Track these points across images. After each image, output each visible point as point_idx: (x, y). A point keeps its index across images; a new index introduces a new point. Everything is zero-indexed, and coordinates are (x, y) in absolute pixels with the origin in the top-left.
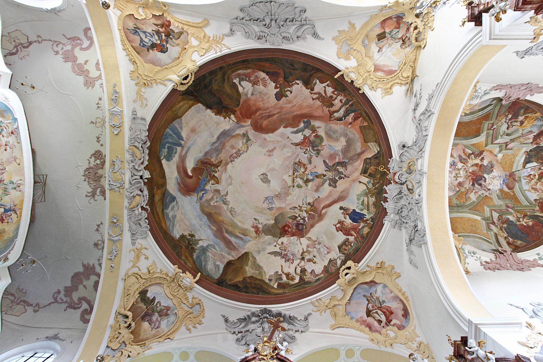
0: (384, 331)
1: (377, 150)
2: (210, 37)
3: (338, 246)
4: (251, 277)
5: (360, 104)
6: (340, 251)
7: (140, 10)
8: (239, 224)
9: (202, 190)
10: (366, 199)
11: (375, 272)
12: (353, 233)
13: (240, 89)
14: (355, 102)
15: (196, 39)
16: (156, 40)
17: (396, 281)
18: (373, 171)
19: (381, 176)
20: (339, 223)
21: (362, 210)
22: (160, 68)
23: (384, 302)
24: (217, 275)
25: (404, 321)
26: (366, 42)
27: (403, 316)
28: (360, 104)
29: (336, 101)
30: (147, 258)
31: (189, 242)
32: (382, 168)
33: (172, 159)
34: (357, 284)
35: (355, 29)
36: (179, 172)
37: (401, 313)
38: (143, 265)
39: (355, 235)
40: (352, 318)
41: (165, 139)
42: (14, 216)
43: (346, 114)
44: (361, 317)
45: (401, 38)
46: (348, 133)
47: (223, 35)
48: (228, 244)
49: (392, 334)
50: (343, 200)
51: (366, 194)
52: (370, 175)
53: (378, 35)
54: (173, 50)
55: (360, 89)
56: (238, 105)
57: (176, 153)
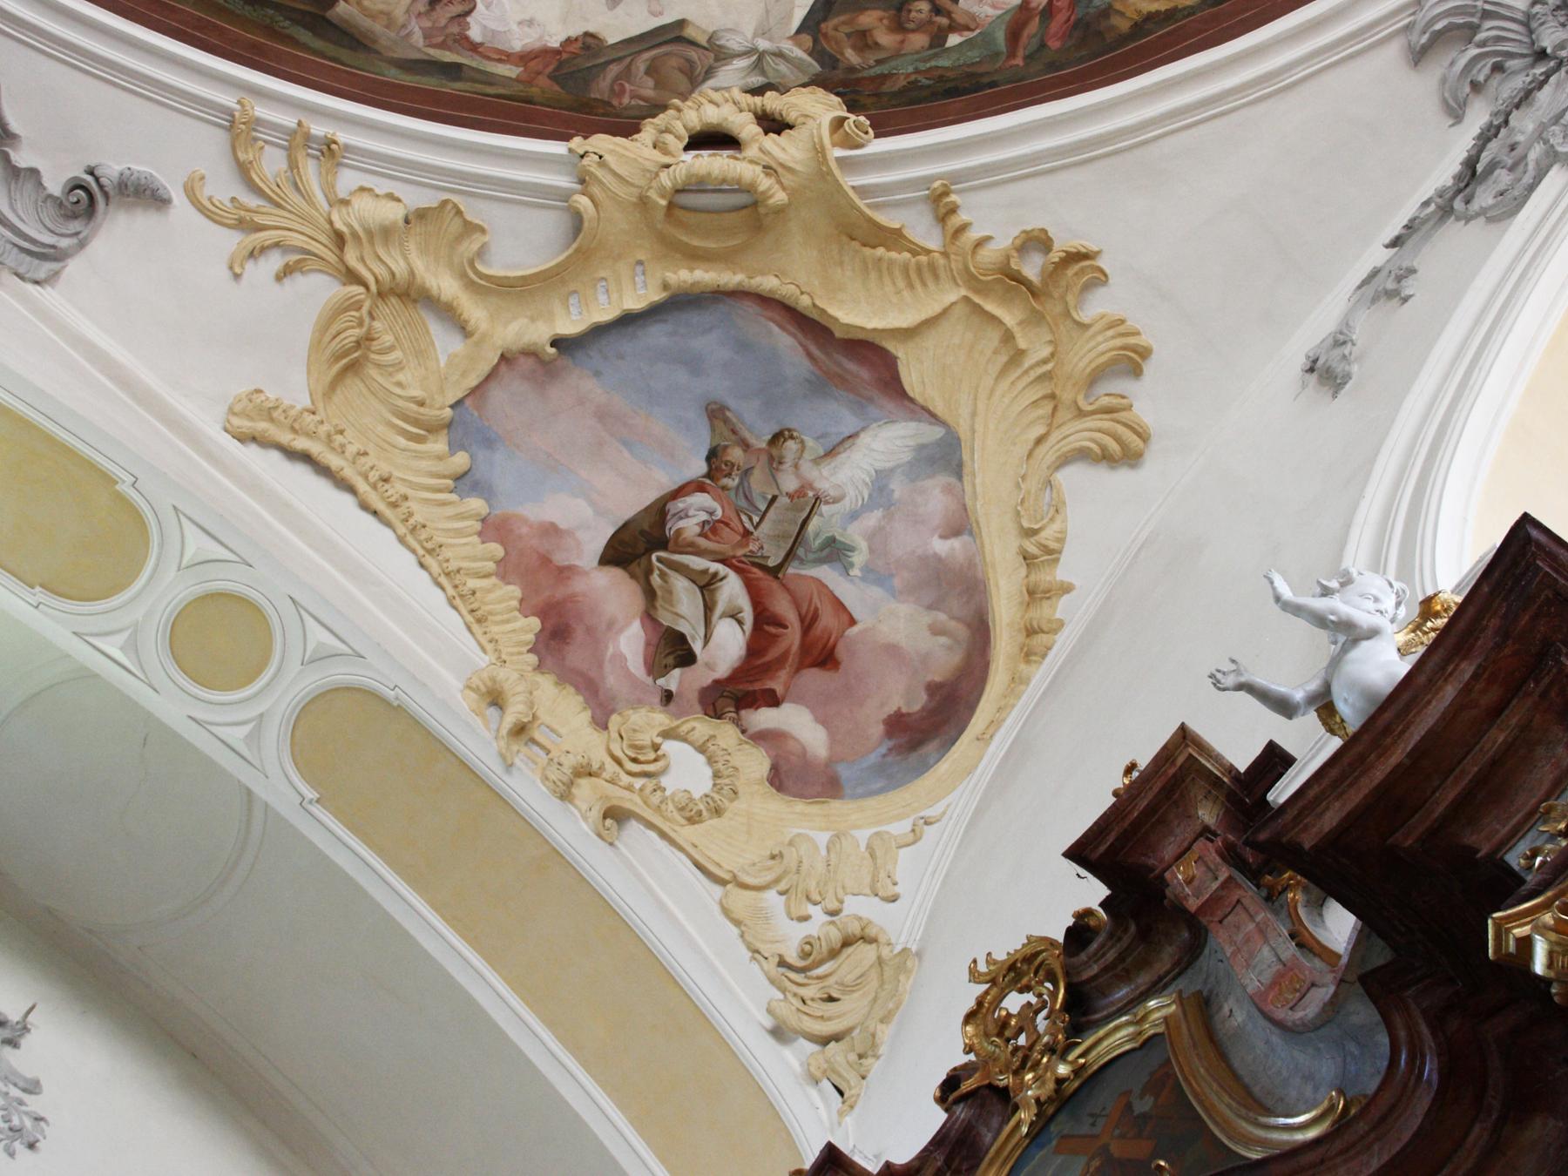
0: (648, 721)
11: (953, 295)
17: (1073, 478)
23: (835, 551)
25: (873, 758)
27: (897, 724)
34: (730, 278)
40: (464, 482)
44: (551, 531)
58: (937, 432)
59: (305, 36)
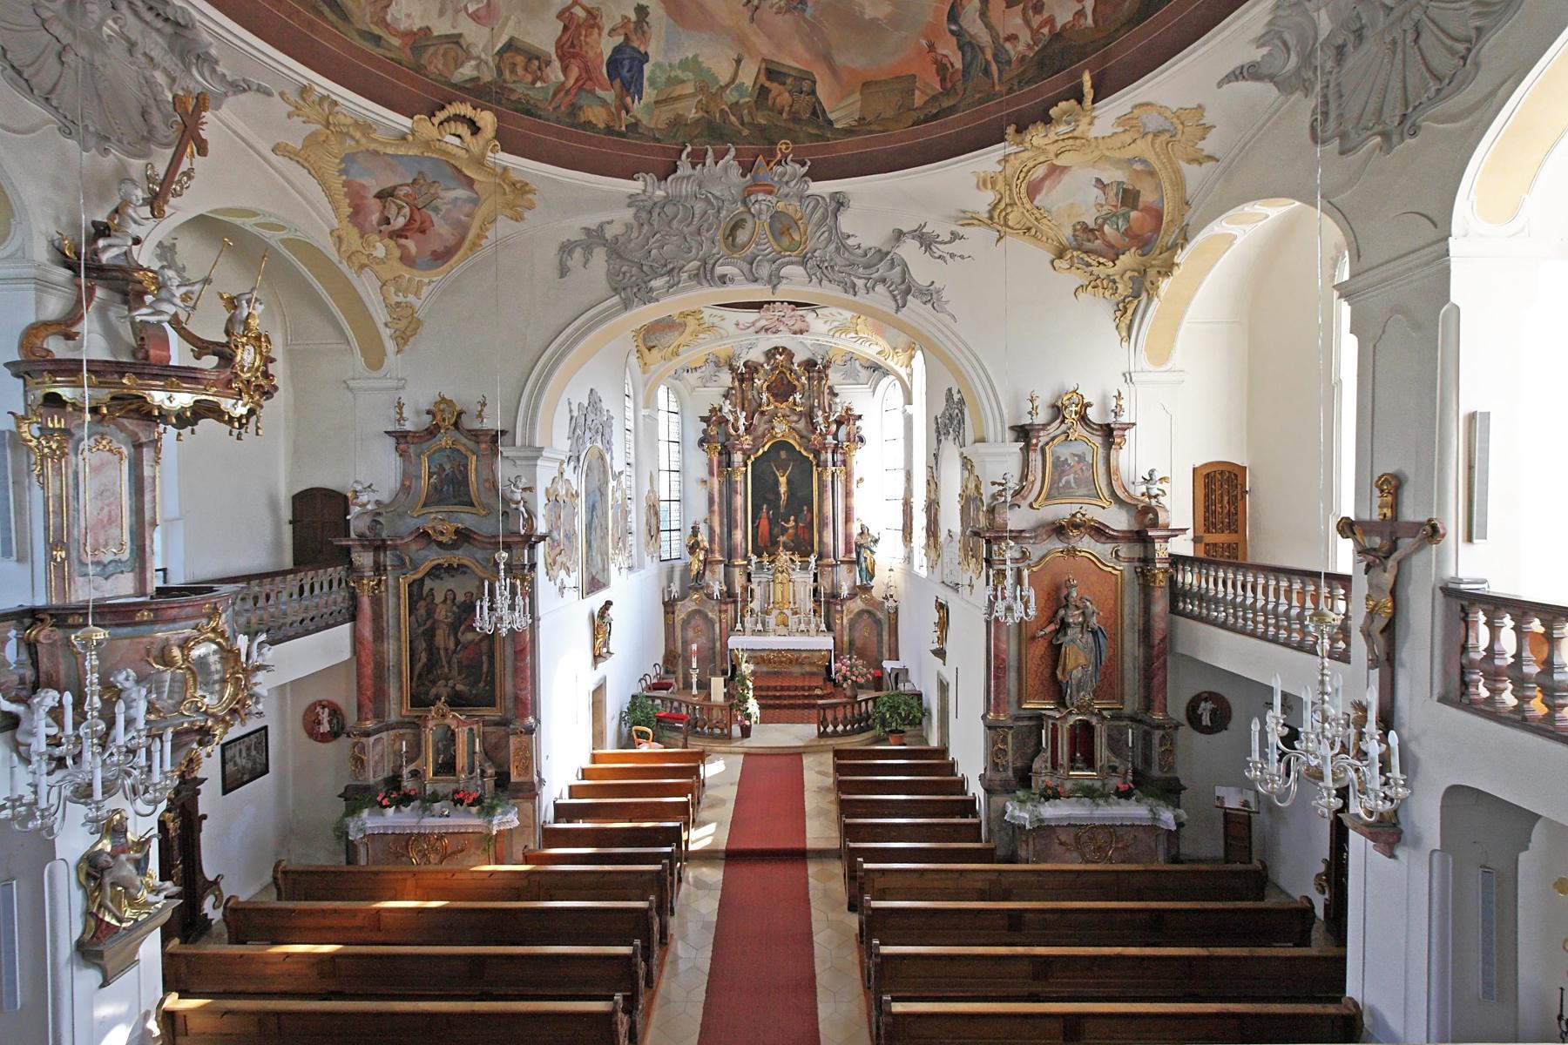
1: (838, 120)
3: (512, 39)
5: (981, 102)
6: (500, 53)
10: (689, 89)
12: (575, 72)
14: (993, 86)
18: (775, 99)
19: (762, 129)
20: (589, 12)
21: (652, 84)
23: (436, 210)
26: (1138, 167)
27: (434, 253)
28: (981, 102)
29: (1019, 21)
32: (784, 147)
35: (1191, 161)
37: (437, 246)
39: (571, 81)
43: (966, 44)
44: (363, 186)
45: (1101, 229)
46: (903, 34)
49: (380, 252)
50: (670, 15)
51: (702, 89)
52: (763, 92)
53: (1137, 194)
55: (1019, 131)
58: (475, 196)
59: (326, 11)
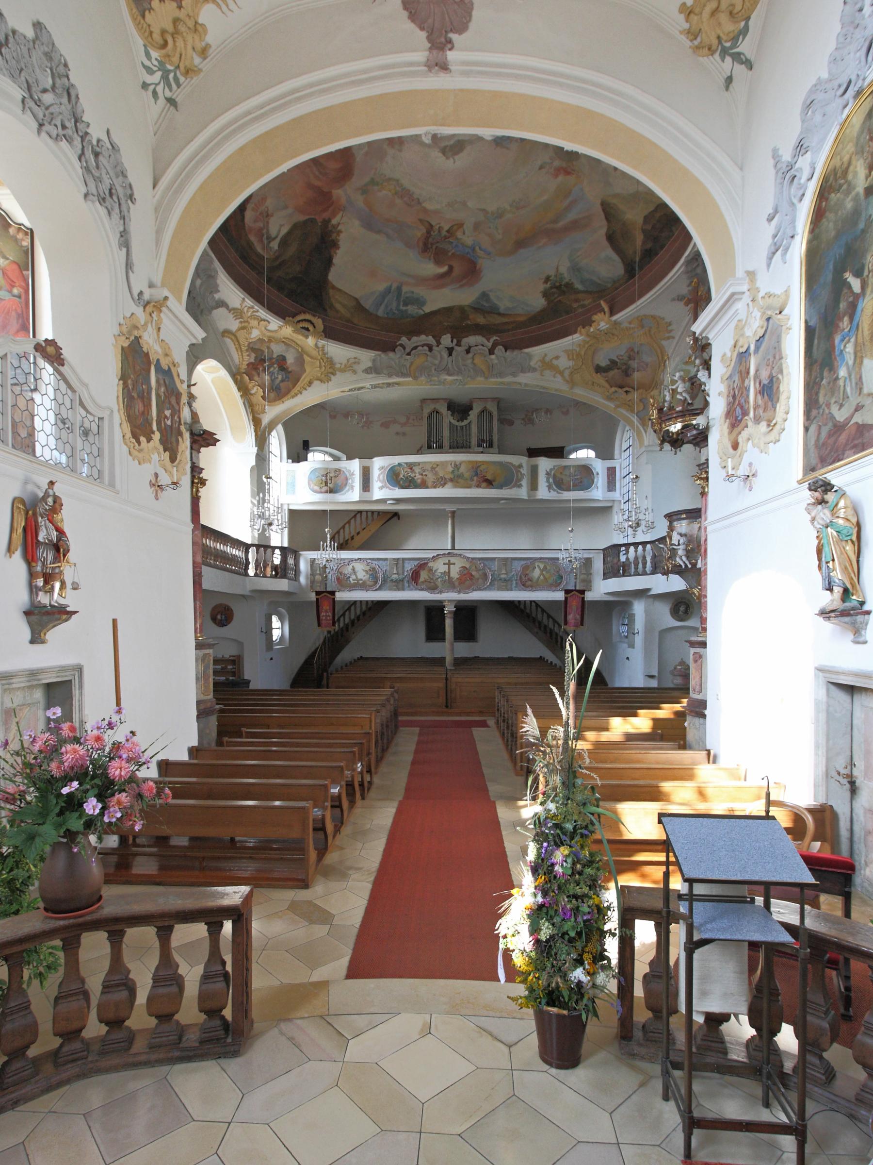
2: (241, 322)
4: (646, 219)
7: (253, 392)
8: (545, 197)
9: (474, 250)
13: (284, 231)
15: (251, 333)
16: (275, 368)
22: (305, 356)
24: (619, 269)
30: (557, 358)
31: (557, 288)
33: (422, 297)
36: (442, 286)
38: (564, 363)
41: (394, 313)
42: (482, 467)
47: (230, 312)
48: (575, 226)
54: (277, 349)
56: (312, 221)
57: (413, 292)
